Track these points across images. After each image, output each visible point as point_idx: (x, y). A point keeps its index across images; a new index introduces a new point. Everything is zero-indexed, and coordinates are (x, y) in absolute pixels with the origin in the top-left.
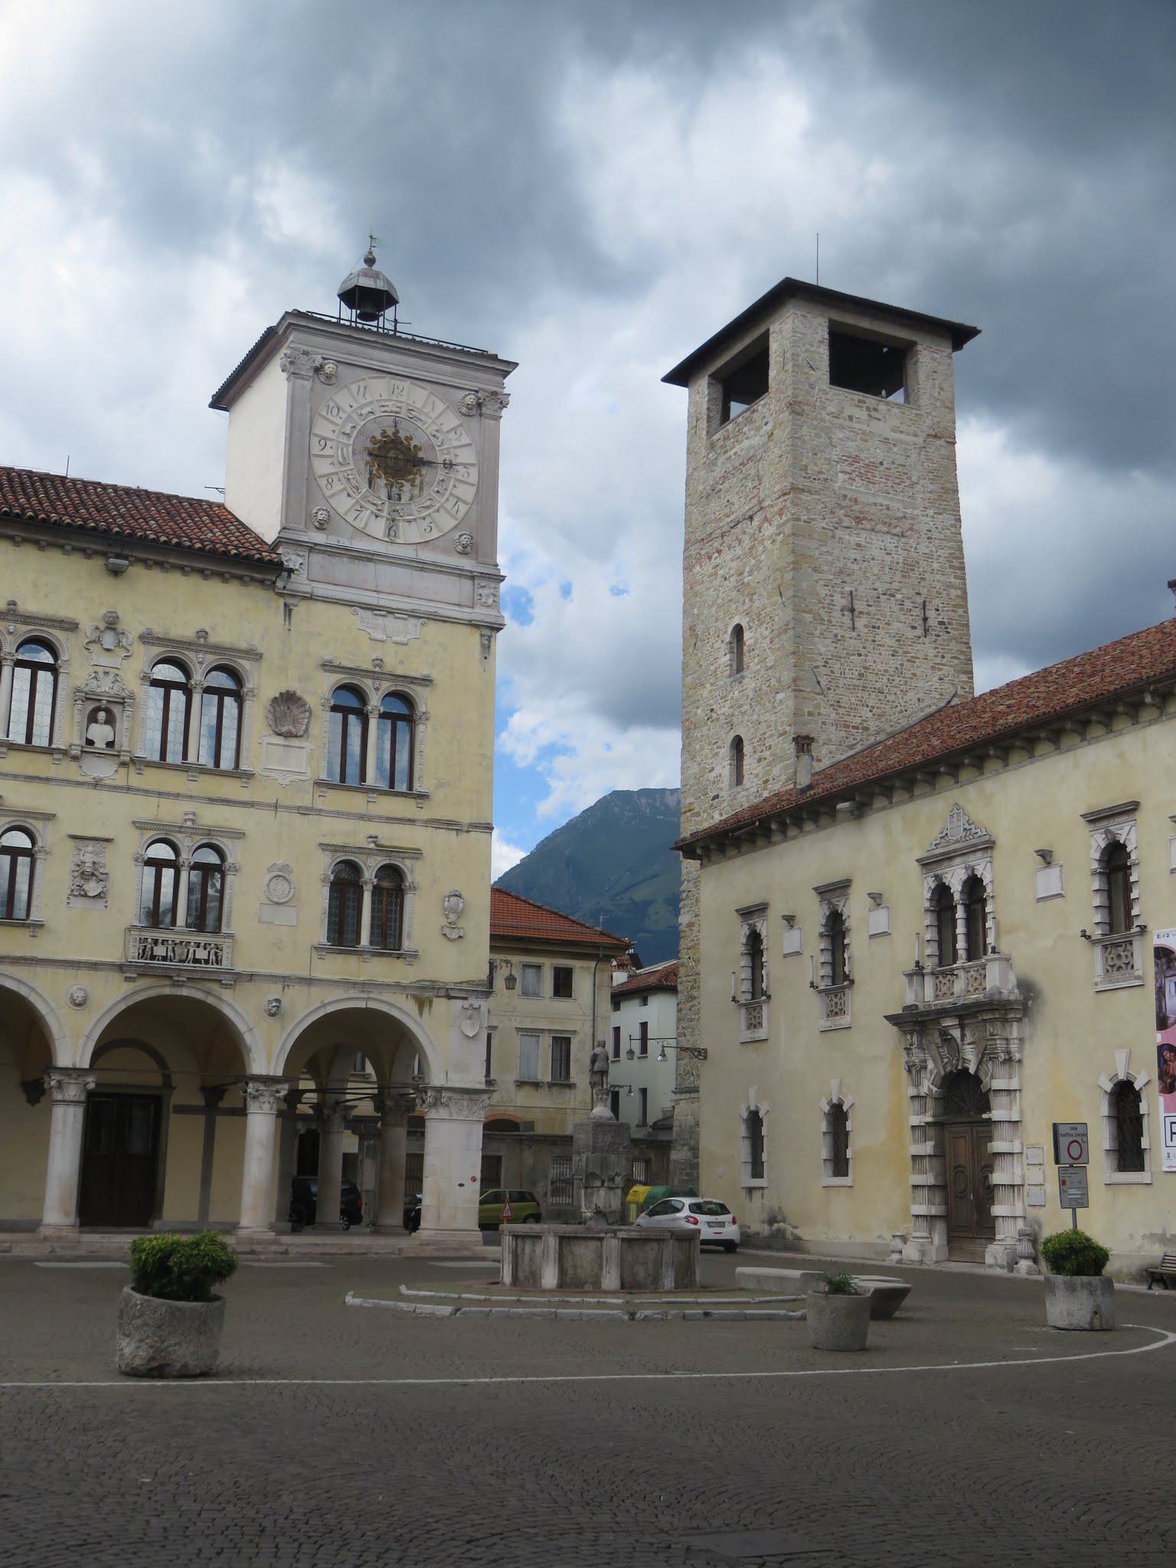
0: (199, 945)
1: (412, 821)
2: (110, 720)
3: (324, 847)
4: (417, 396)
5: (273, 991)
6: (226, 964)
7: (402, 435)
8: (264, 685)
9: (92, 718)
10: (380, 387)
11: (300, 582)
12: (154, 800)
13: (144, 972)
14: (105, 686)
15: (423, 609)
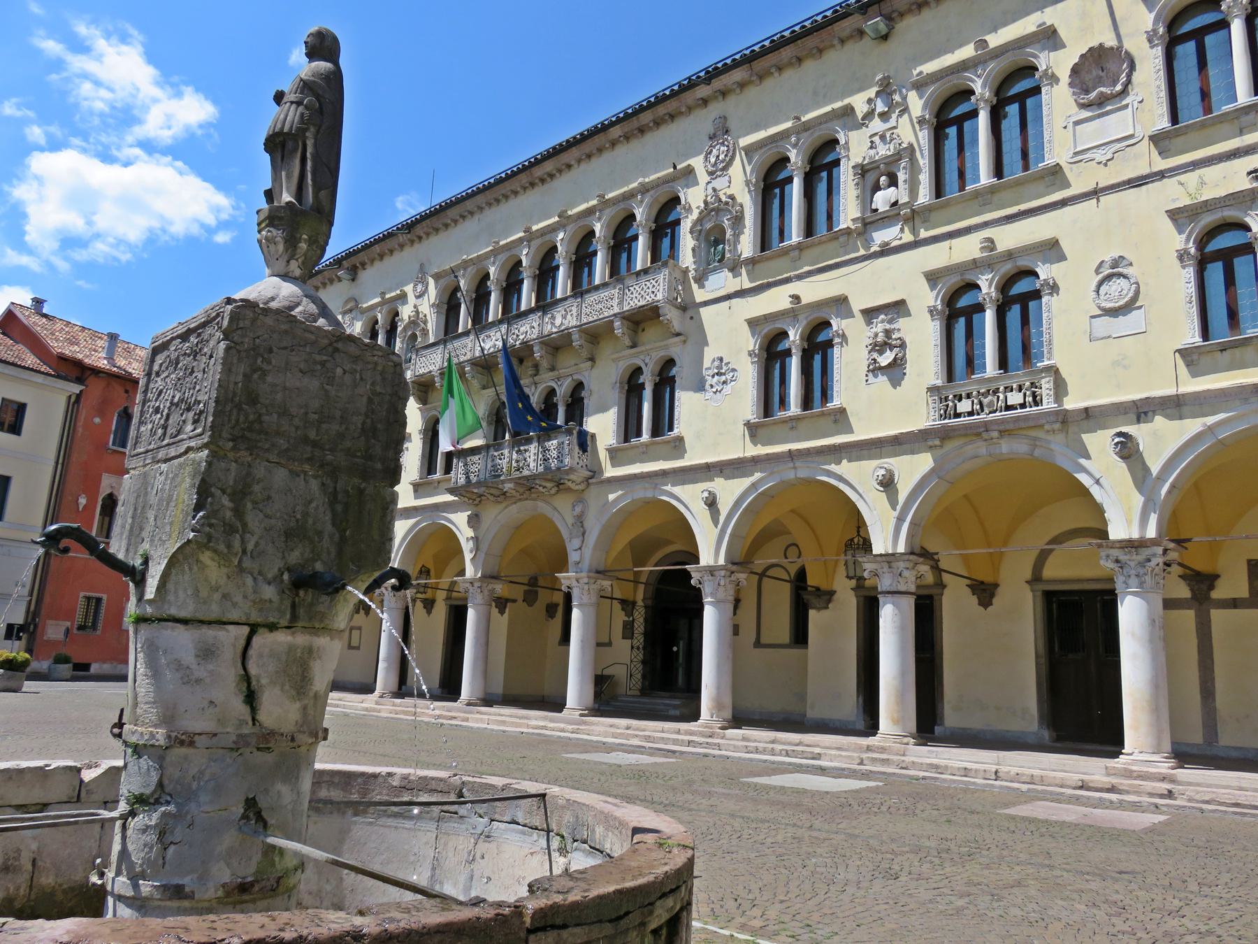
2: (893, 182)
6: (1048, 404)
9: (877, 188)
14: (883, 151)
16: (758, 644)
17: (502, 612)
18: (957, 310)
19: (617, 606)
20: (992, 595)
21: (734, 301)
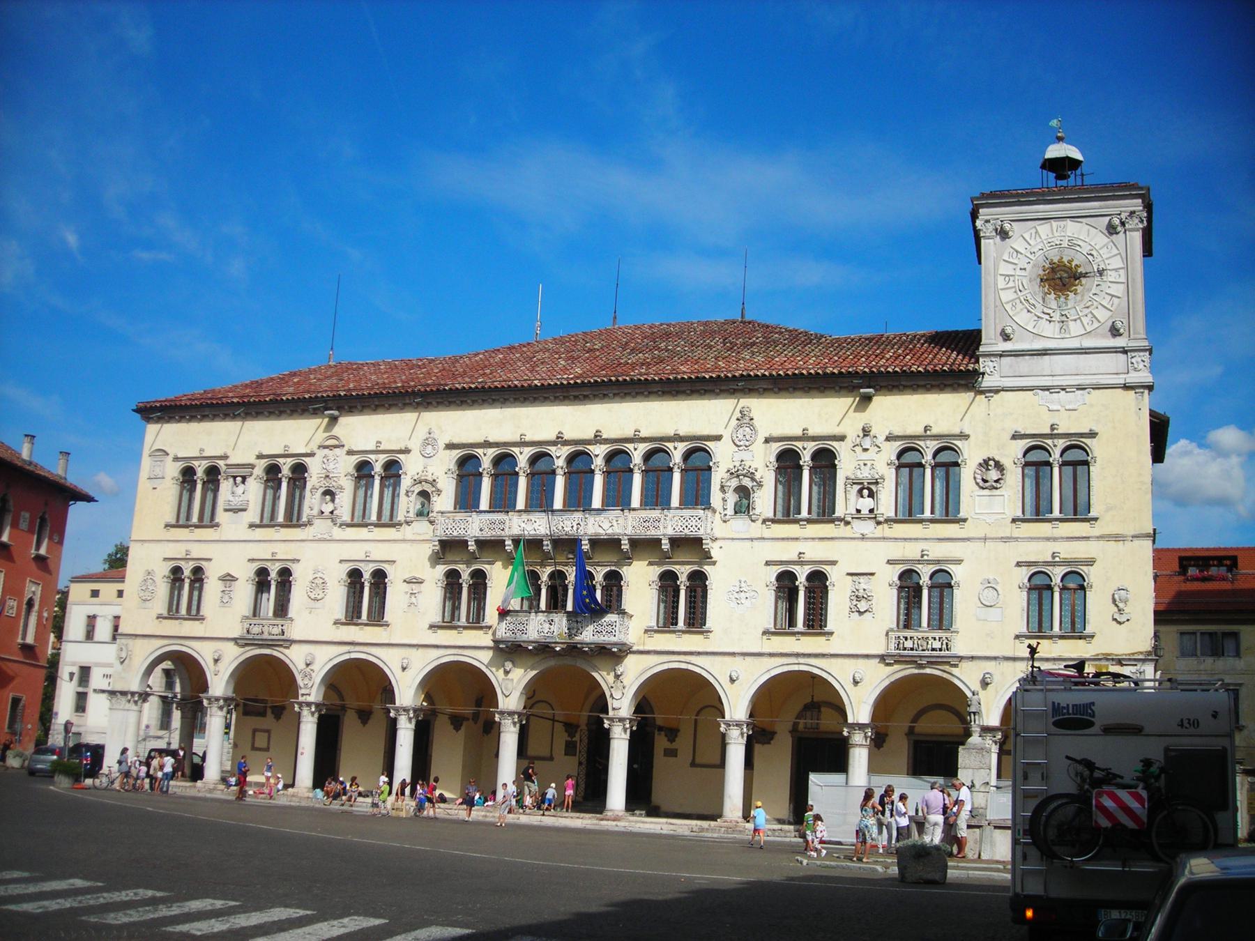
0: (934, 639)
1: (1087, 538)
3: (1018, 564)
4: (1072, 228)
5: (989, 666)
7: (1065, 260)
8: (971, 456)
10: (1044, 229)
11: (987, 382)
12: (901, 544)
13: (899, 660)
14: (865, 474)
15: (1088, 382)
16: (693, 764)
17: (457, 728)
18: (908, 586)
19: (559, 727)
20: (884, 741)
21: (756, 543)
